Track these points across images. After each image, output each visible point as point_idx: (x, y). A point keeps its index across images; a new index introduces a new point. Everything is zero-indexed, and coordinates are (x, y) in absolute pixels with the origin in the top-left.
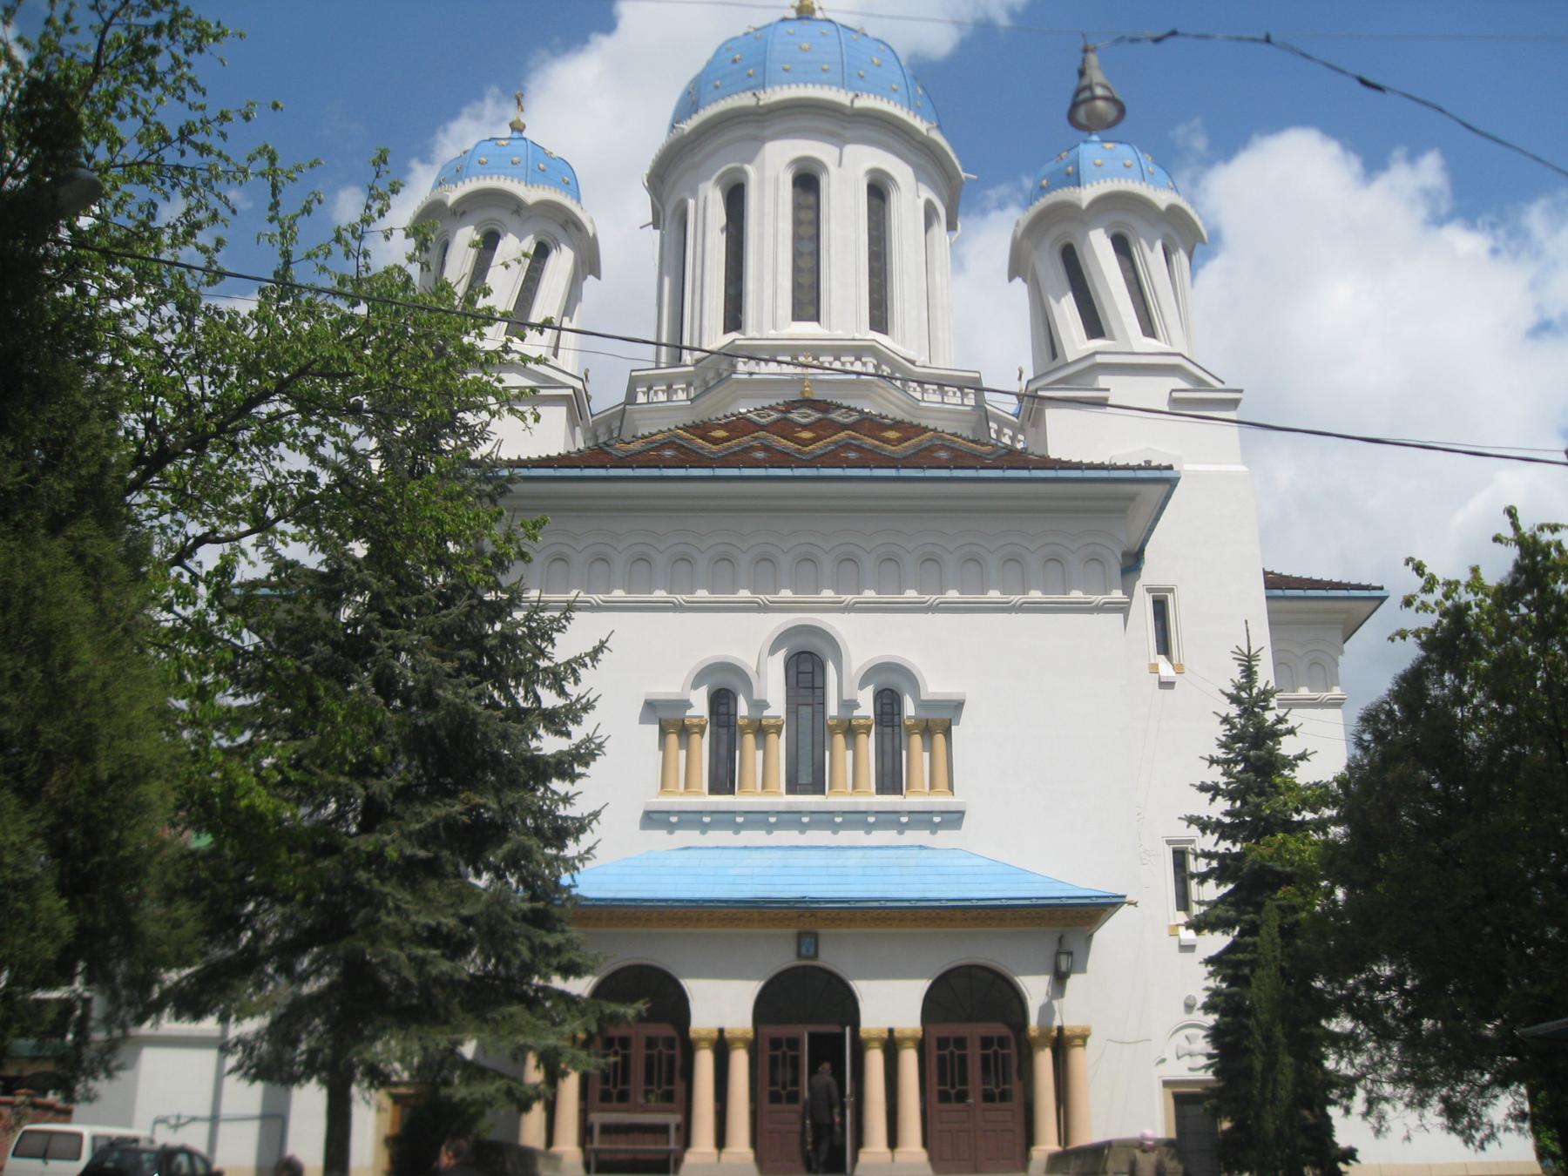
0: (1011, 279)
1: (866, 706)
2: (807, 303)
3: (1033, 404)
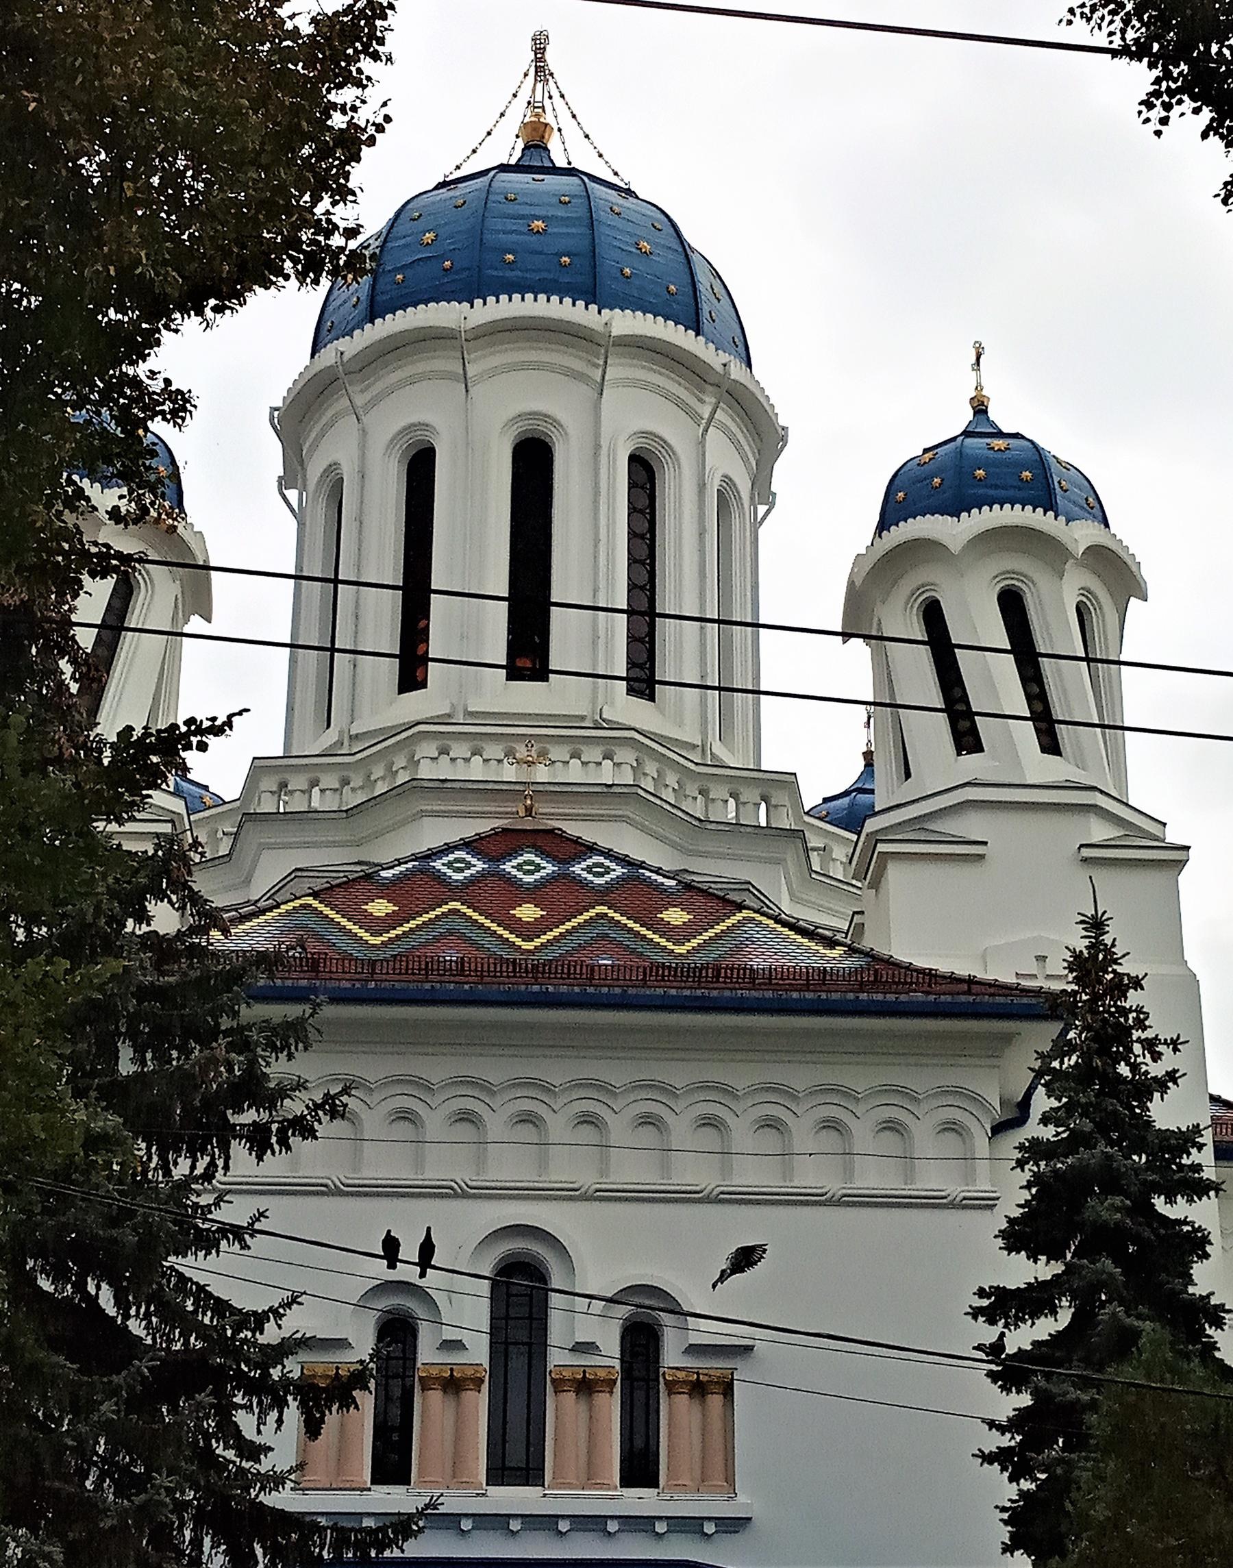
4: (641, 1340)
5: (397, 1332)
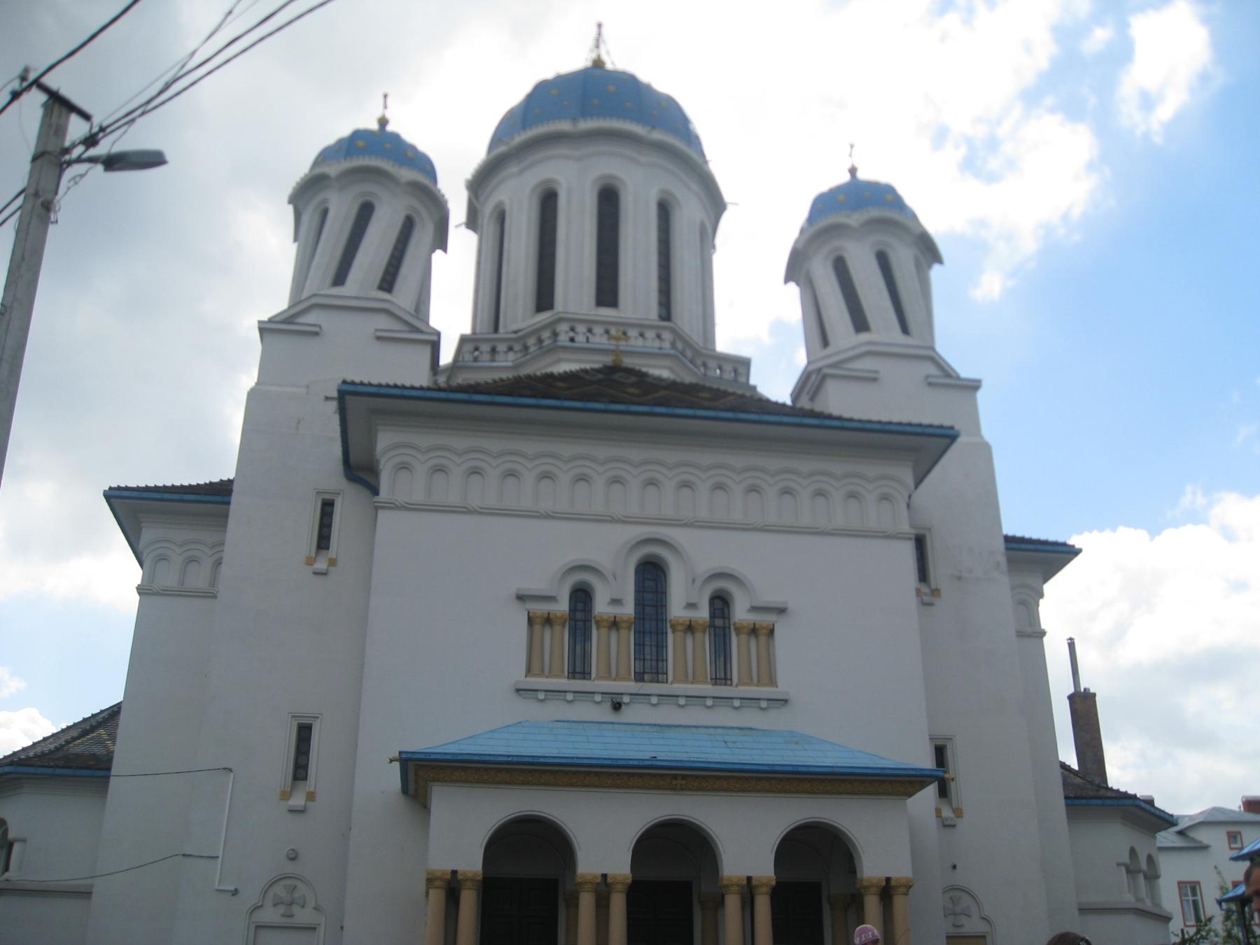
0: (787, 280)
1: (703, 613)
2: (607, 292)
3: (810, 382)
4: (721, 603)
5: (582, 596)
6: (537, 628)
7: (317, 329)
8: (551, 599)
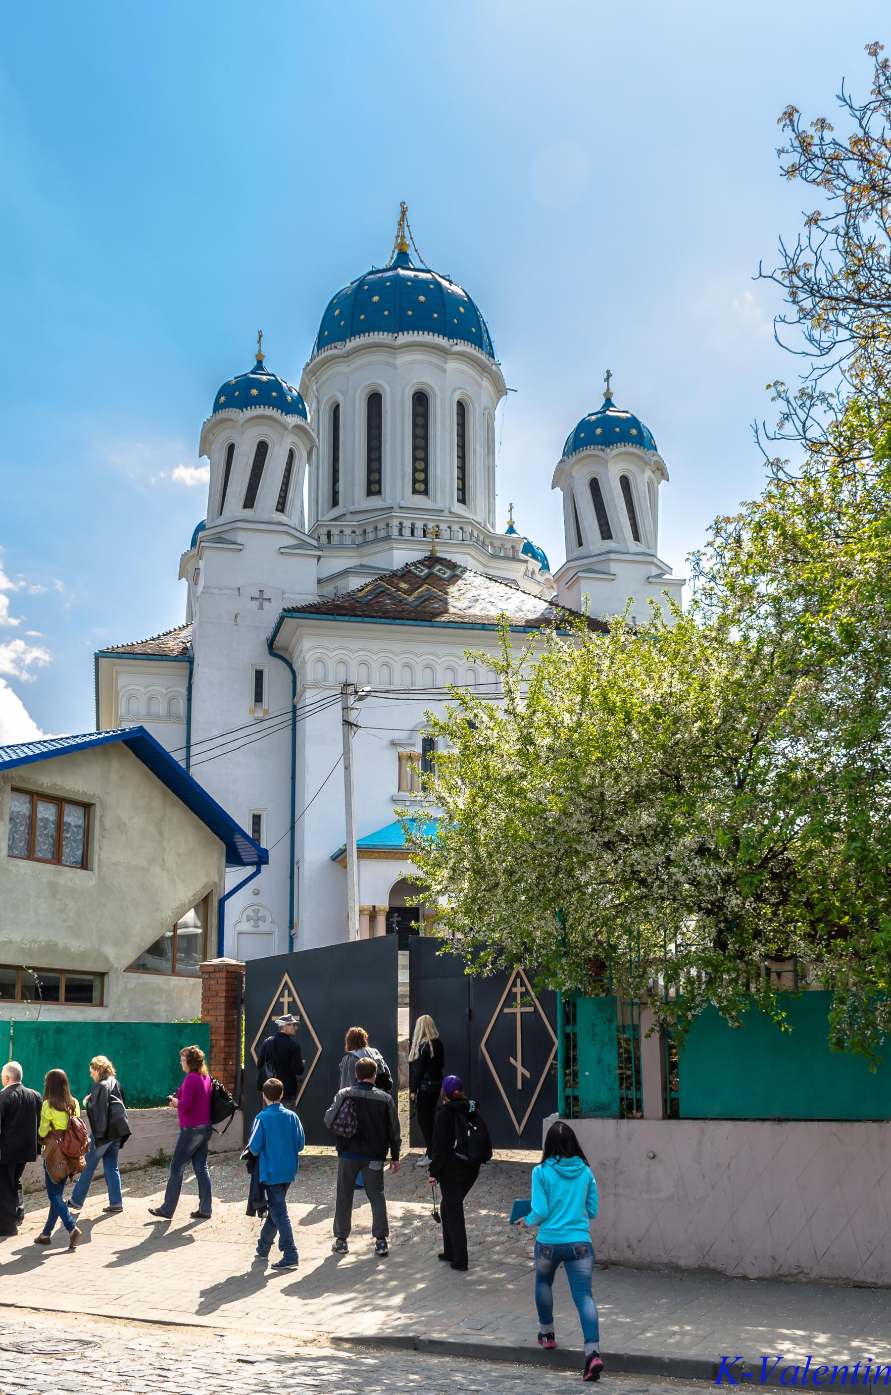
5: (429, 744)
6: (404, 762)
7: (241, 547)
8: (413, 745)
